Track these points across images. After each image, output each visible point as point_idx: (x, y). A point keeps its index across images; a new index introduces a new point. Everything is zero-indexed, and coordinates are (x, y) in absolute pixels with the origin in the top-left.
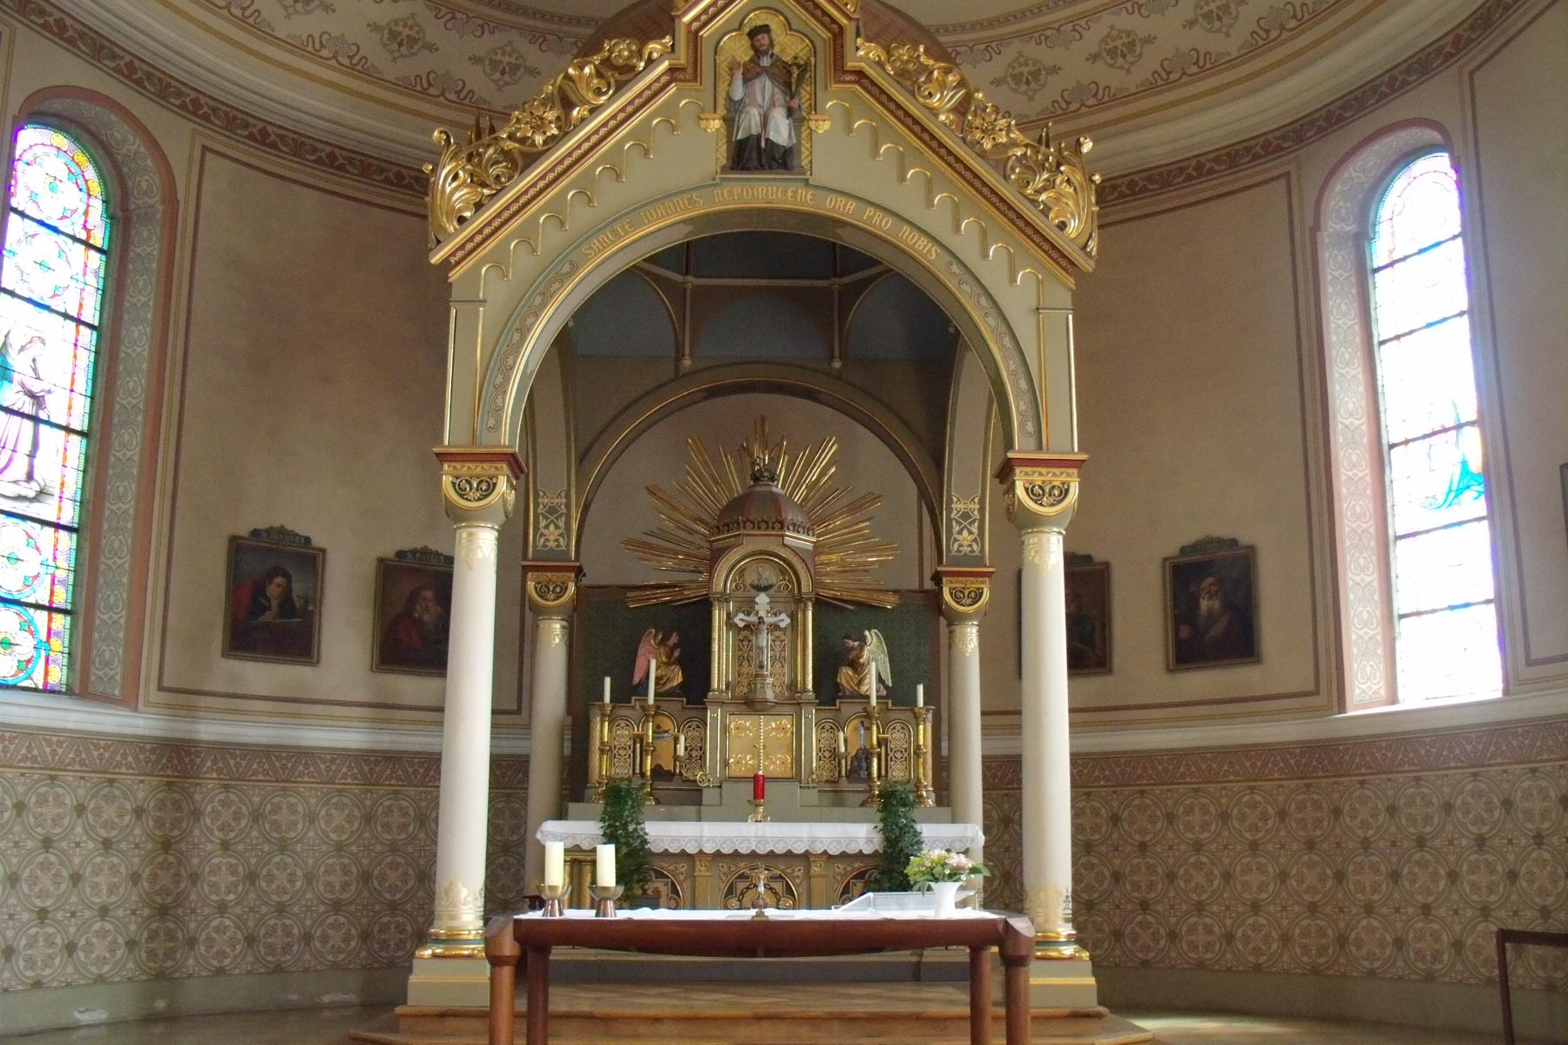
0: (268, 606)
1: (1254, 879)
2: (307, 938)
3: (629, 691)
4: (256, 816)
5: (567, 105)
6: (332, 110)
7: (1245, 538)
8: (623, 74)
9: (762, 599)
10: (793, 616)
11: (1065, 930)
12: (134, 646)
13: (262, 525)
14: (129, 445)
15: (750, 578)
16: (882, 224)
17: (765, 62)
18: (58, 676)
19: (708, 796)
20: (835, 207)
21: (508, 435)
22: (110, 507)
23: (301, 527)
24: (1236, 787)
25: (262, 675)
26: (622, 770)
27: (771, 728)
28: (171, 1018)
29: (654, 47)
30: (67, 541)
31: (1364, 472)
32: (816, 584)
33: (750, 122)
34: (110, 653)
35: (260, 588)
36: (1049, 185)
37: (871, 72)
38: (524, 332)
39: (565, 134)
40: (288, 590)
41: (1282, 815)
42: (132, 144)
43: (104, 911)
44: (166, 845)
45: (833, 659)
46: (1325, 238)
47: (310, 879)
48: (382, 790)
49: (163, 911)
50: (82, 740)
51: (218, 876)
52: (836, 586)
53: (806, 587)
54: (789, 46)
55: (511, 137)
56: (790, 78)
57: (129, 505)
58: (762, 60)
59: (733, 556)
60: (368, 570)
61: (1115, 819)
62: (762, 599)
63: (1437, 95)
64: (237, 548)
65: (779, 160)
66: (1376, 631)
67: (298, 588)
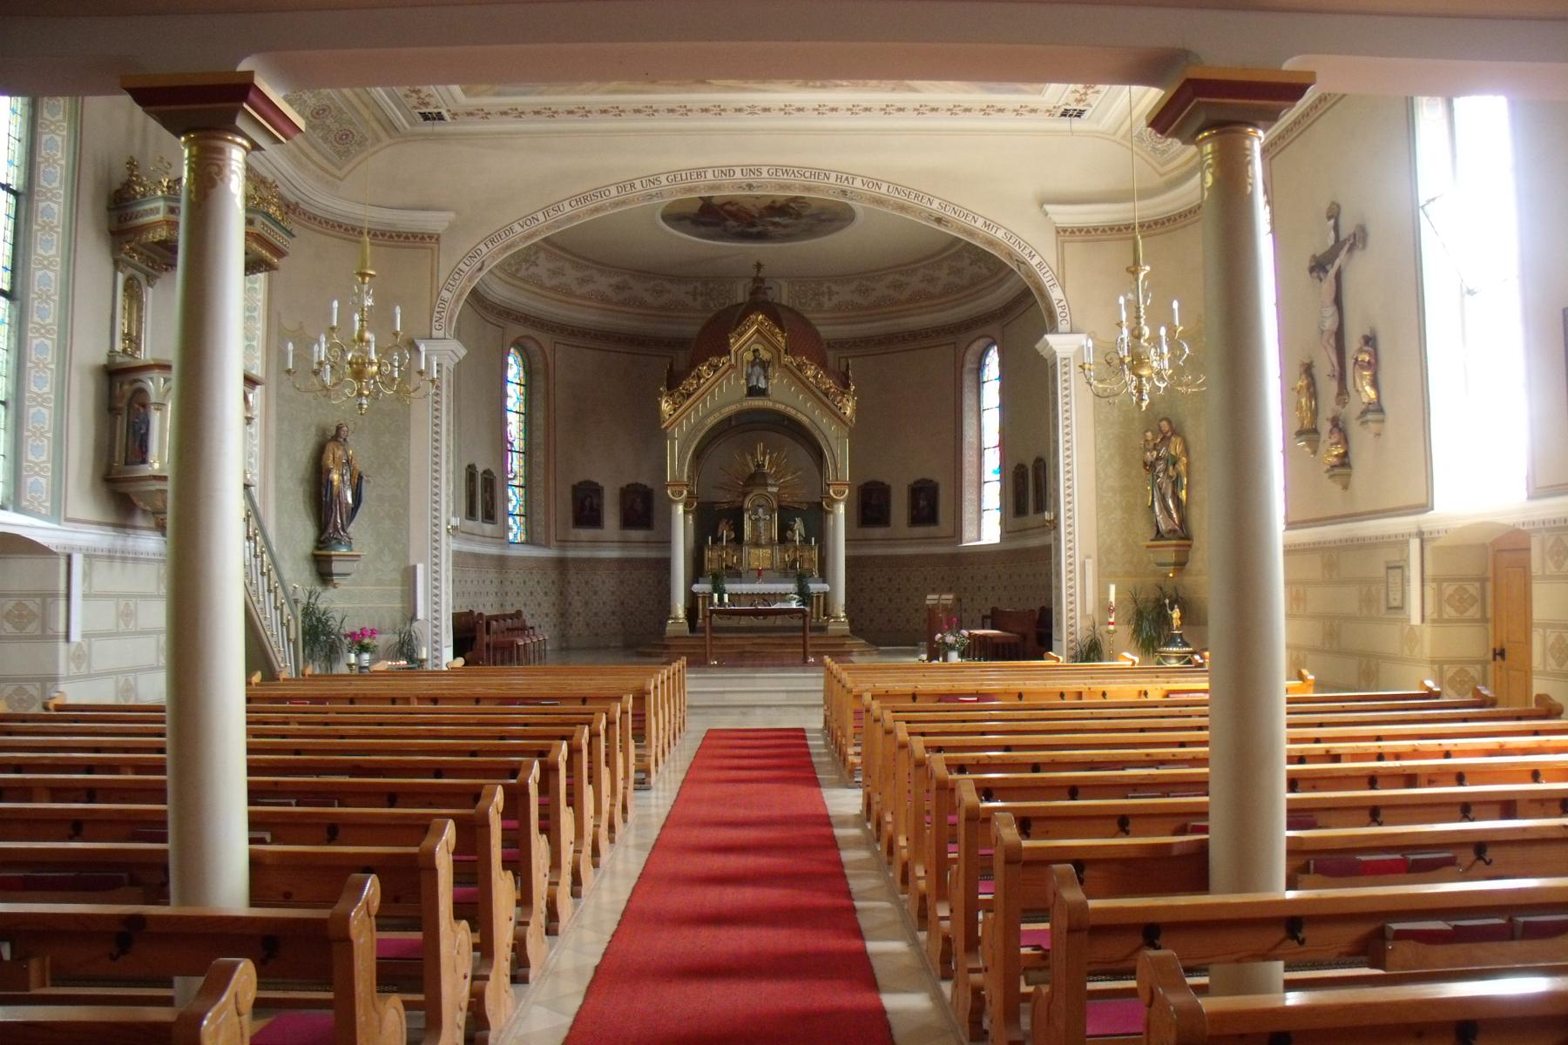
0: (586, 510)
5: (699, 378)
7: (937, 478)
12: (547, 527)
14: (539, 456)
16: (793, 412)
20: (781, 407)
23: (595, 479)
25: (585, 533)
26: (715, 566)
27: (764, 553)
31: (975, 459)
34: (539, 529)
42: (531, 346)
45: (785, 528)
46: (966, 369)
49: (562, 615)
50: (537, 559)
51: (577, 604)
52: (787, 499)
56: (765, 365)
58: (757, 361)
60: (617, 491)
63: (993, 329)
64: (575, 488)
65: (762, 393)
66: (975, 516)
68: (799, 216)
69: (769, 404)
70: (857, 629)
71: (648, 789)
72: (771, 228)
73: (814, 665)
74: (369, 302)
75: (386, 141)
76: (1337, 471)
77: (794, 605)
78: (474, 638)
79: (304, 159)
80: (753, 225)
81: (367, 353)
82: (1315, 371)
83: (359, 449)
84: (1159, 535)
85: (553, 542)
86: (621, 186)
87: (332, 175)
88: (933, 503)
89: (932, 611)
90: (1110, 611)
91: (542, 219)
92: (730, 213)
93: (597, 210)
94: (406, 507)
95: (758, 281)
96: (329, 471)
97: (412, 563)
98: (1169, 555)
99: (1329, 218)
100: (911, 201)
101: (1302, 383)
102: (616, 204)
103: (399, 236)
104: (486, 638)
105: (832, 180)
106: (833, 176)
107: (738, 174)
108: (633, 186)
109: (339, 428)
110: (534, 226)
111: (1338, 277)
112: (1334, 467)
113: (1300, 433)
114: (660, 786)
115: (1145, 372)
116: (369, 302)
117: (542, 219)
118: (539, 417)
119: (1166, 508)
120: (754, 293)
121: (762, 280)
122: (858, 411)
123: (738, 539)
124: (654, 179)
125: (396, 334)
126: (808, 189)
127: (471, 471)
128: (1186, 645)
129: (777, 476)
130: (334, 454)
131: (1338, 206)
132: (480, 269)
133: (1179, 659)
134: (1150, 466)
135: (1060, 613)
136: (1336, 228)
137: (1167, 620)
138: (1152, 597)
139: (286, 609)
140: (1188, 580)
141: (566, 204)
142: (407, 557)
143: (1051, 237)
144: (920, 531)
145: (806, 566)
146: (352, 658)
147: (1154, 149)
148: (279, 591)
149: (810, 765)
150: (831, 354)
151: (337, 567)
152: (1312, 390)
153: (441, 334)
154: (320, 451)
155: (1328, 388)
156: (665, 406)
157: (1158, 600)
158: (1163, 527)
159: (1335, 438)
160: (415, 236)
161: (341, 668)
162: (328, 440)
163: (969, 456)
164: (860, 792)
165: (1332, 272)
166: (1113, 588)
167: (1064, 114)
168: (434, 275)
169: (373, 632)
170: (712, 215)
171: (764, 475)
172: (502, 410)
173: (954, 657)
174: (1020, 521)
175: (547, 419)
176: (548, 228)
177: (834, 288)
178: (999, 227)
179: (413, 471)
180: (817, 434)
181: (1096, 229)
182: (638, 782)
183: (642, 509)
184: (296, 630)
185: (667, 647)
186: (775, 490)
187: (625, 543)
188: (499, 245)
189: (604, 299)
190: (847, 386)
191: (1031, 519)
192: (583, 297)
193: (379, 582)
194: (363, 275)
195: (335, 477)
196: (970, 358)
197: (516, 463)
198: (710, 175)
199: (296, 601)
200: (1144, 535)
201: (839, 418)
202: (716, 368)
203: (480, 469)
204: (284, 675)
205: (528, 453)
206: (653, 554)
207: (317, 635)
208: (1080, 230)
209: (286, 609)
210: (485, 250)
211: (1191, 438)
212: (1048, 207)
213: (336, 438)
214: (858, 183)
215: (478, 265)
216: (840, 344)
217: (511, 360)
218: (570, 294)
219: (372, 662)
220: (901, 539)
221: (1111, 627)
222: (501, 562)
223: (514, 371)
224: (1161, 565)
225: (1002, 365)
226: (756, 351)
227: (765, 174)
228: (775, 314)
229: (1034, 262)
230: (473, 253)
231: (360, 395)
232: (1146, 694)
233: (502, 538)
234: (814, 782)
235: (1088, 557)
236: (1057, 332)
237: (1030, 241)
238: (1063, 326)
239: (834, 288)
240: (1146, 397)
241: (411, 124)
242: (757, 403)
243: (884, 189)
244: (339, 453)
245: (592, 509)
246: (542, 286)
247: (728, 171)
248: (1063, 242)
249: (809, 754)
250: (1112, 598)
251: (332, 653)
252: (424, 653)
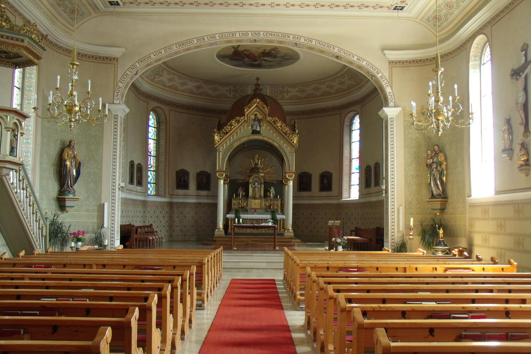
0: (182, 181)
2: (189, 231)
3: (237, 195)
4: (181, 213)
5: (231, 126)
7: (331, 171)
9: (256, 183)
11: (291, 228)
14: (162, 158)
16: (271, 141)
18: (155, 193)
19: (249, 211)
20: (266, 139)
22: (160, 168)
23: (185, 169)
25: (182, 192)
27: (257, 201)
28: (172, 241)
30: (154, 173)
31: (348, 163)
34: (162, 189)
38: (226, 156)
41: (333, 214)
42: (160, 111)
43: (164, 226)
44: (170, 217)
45: (266, 191)
46: (345, 125)
47: (189, 222)
49: (170, 226)
50: (160, 202)
52: (268, 179)
53: (263, 182)
54: (260, 117)
56: (259, 121)
57: (163, 167)
58: (256, 119)
59: (252, 177)
60: (196, 174)
61: (311, 214)
62: (256, 183)
63: (357, 108)
64: (177, 173)
65: (258, 133)
66: (348, 187)
67: (186, 178)
68: (275, 57)
69: (261, 138)
70: (297, 235)
71: (203, 309)
72: (263, 62)
73: (279, 250)
74: (76, 77)
75: (94, 14)
76: (523, 167)
77: (270, 224)
78: (130, 236)
79: (55, 20)
80: (255, 61)
81: (74, 101)
82: (512, 122)
83: (80, 152)
84: (433, 196)
85: (167, 195)
86: (198, 39)
87: (70, 29)
88: (330, 182)
89: (331, 228)
90: (411, 229)
91: (163, 53)
92: (245, 54)
93: (188, 49)
94: (101, 177)
95: (257, 85)
96: (65, 161)
97: (102, 202)
98: (438, 205)
99: (522, 51)
100: (326, 48)
101: (505, 127)
102: (197, 47)
103: (100, 58)
104: (135, 236)
105: (291, 38)
106: (291, 37)
107: (250, 35)
108: (204, 39)
109: (70, 142)
110: (161, 55)
111: (526, 78)
112: (521, 165)
113: (504, 151)
114: (209, 307)
115: (440, 118)
116: (76, 77)
117: (163, 53)
118: (163, 141)
119: (436, 184)
120: (255, 90)
121: (259, 85)
122: (299, 141)
123: (247, 196)
124: (213, 36)
125: (88, 93)
126: (281, 42)
127: (132, 164)
128: (446, 245)
129: (263, 169)
130: (68, 153)
131: (528, 45)
132: (136, 74)
133: (443, 252)
134: (429, 166)
135: (388, 230)
136: (526, 55)
137: (437, 234)
138: (430, 224)
139: (42, 222)
140: (446, 216)
141: (174, 46)
142: (101, 199)
143: (387, 65)
144: (324, 193)
145: (275, 207)
146: (73, 244)
147: (435, 25)
148: (39, 214)
149: (278, 298)
150: (287, 118)
151: (68, 203)
152: (510, 130)
153: (118, 102)
154: (62, 151)
155: (519, 130)
156: (216, 138)
157: (432, 225)
158: (435, 193)
159: (522, 153)
160: (107, 58)
161: (68, 249)
162: (66, 146)
163: (346, 162)
164: (304, 313)
165: (523, 76)
166: (412, 219)
167: (395, 9)
168: (115, 75)
169: (83, 232)
170: (238, 55)
171: (258, 169)
172: (147, 138)
173: (340, 249)
174: (368, 190)
175: (166, 143)
176: (167, 57)
177: (290, 90)
178: (364, 60)
179: (104, 162)
180: (281, 150)
181: (407, 62)
182: (197, 306)
183: (206, 182)
184: (46, 231)
186: (263, 175)
187: (198, 196)
188: (145, 63)
189: (192, 92)
190: (295, 131)
191: (373, 189)
192: (183, 91)
193: (87, 210)
194: (73, 64)
195: (68, 163)
196: (347, 120)
197: (152, 161)
198: (237, 35)
199: (46, 218)
200: (426, 195)
201: (291, 144)
202: (238, 122)
203: (136, 163)
204: (36, 252)
205: (157, 157)
206: (210, 201)
207: (57, 234)
208: (399, 62)
209: (42, 222)
210: (138, 65)
211: (448, 153)
212: (386, 52)
213: (69, 146)
214: (302, 40)
215: (135, 72)
216: (292, 113)
217: (151, 117)
218: (176, 89)
219: (82, 246)
220: (316, 197)
221: (411, 237)
222: (144, 203)
223: (152, 121)
224: (434, 209)
225: (361, 123)
226: (256, 115)
227: (262, 35)
228: (264, 99)
229: (379, 76)
230: (134, 66)
231: (70, 121)
232: (436, 269)
233: (145, 193)
234: (280, 307)
235: (401, 206)
236: (388, 107)
237: (376, 65)
238: (391, 104)
239: (290, 90)
240: (441, 130)
241: (105, 7)
242: (256, 137)
243: (314, 43)
244: (71, 152)
246: (165, 86)
247: (246, 33)
248: (392, 67)
249: (277, 292)
250: (412, 224)
251: (64, 242)
252: (106, 243)
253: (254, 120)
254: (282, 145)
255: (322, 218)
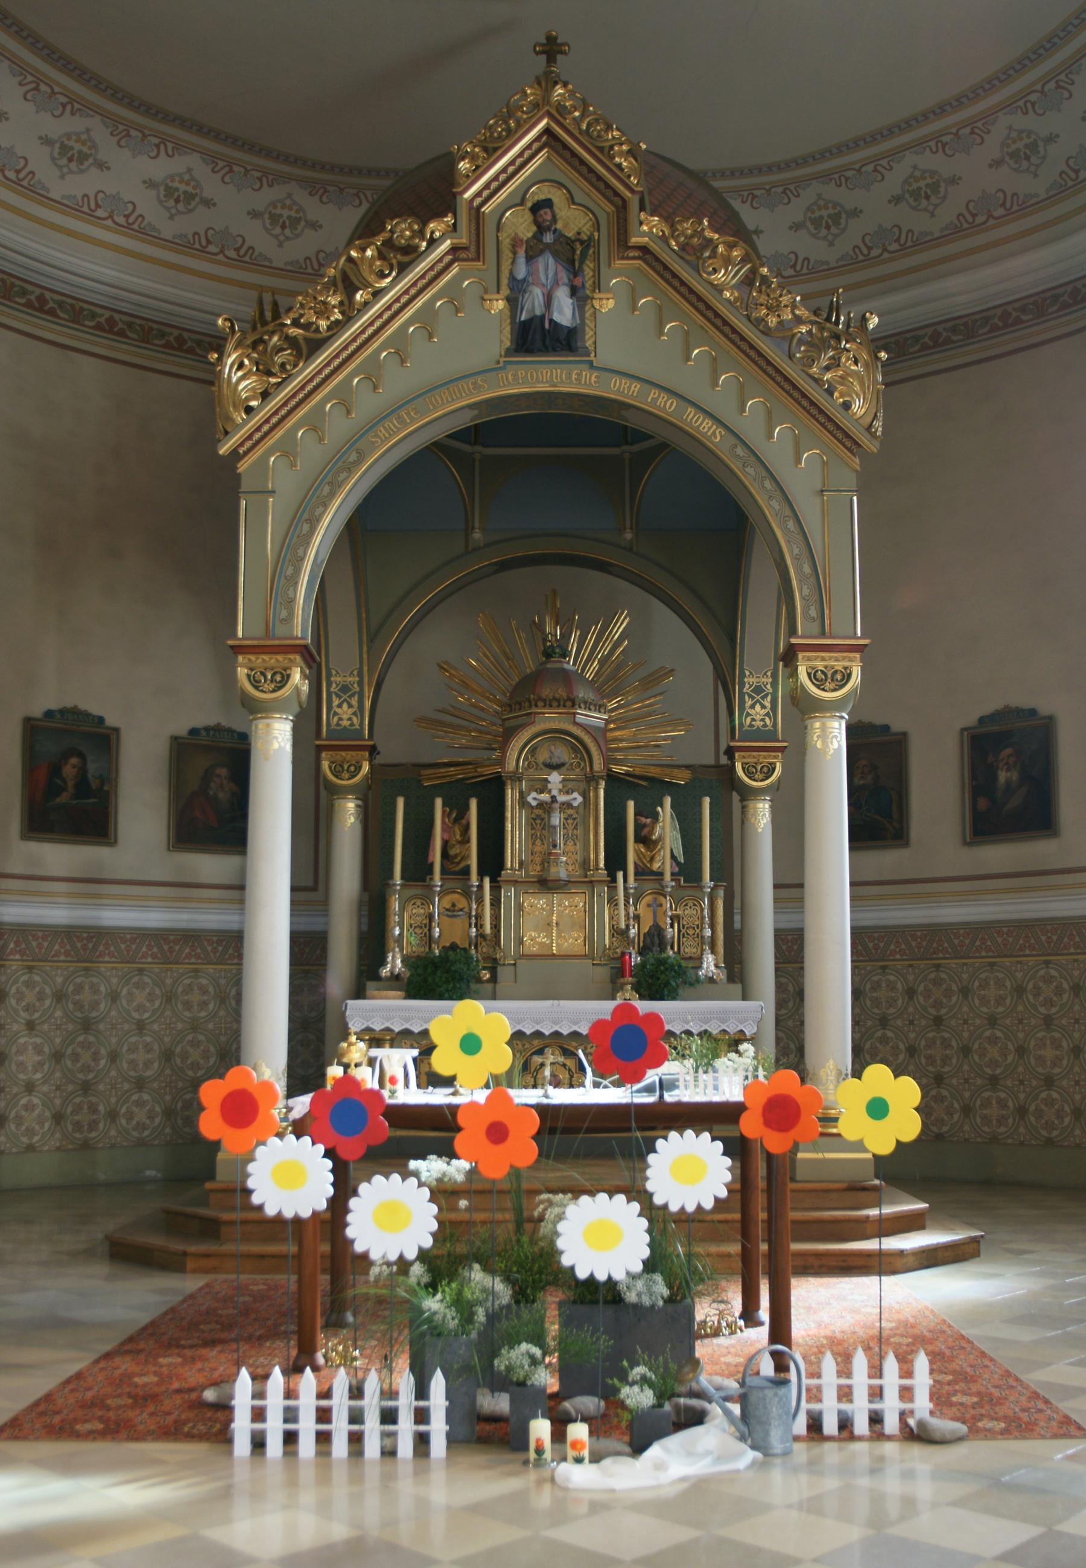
1: (1049, 1053)
5: (350, 289)
6: (109, 273)
7: (1044, 709)
8: (403, 256)
10: (585, 795)
13: (53, 705)
15: (543, 756)
16: (666, 405)
17: (548, 238)
21: (300, 625)
23: (95, 710)
24: (1031, 961)
25: (58, 856)
27: (568, 906)
29: (436, 227)
32: (608, 761)
33: (534, 302)
35: (56, 770)
36: (834, 364)
37: (655, 247)
38: (314, 522)
39: (348, 319)
40: (83, 771)
48: (181, 968)
53: (598, 765)
54: (572, 221)
55: (296, 323)
56: (573, 255)
58: (546, 239)
60: (160, 749)
64: (32, 729)
67: (92, 768)
144: (999, 855)
171: (566, 678)
185: (210, 1229)
189: (135, 226)
245: (83, 786)
253: (533, 250)
254: (753, 433)
255: (992, 1021)
